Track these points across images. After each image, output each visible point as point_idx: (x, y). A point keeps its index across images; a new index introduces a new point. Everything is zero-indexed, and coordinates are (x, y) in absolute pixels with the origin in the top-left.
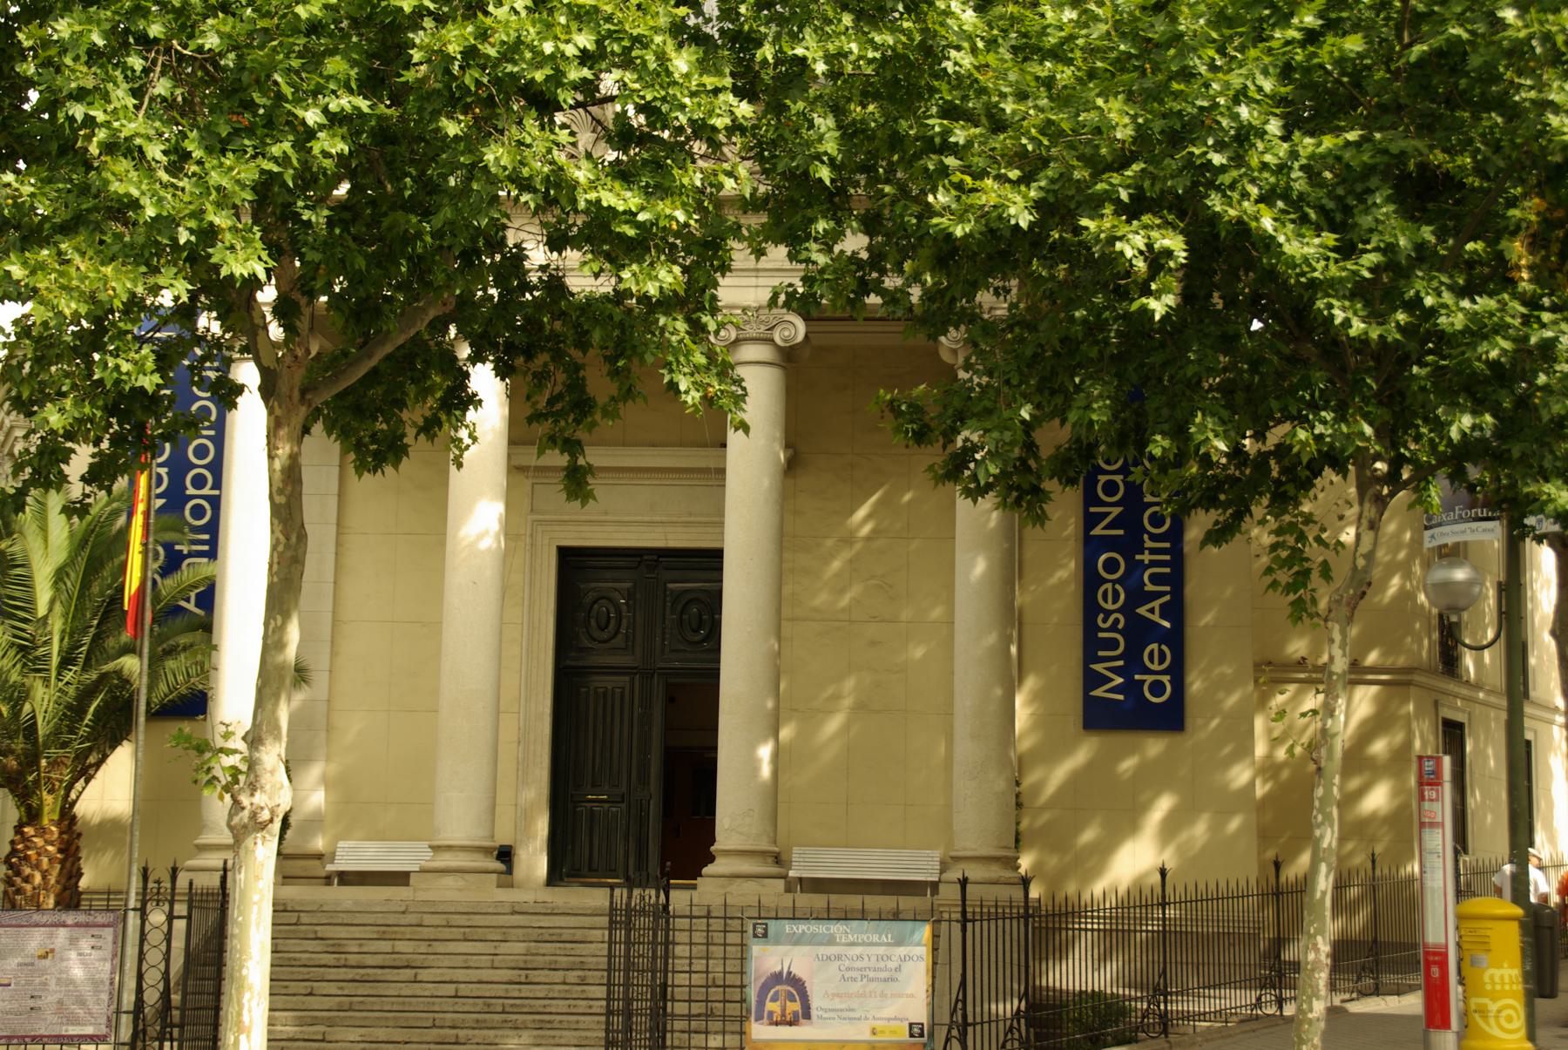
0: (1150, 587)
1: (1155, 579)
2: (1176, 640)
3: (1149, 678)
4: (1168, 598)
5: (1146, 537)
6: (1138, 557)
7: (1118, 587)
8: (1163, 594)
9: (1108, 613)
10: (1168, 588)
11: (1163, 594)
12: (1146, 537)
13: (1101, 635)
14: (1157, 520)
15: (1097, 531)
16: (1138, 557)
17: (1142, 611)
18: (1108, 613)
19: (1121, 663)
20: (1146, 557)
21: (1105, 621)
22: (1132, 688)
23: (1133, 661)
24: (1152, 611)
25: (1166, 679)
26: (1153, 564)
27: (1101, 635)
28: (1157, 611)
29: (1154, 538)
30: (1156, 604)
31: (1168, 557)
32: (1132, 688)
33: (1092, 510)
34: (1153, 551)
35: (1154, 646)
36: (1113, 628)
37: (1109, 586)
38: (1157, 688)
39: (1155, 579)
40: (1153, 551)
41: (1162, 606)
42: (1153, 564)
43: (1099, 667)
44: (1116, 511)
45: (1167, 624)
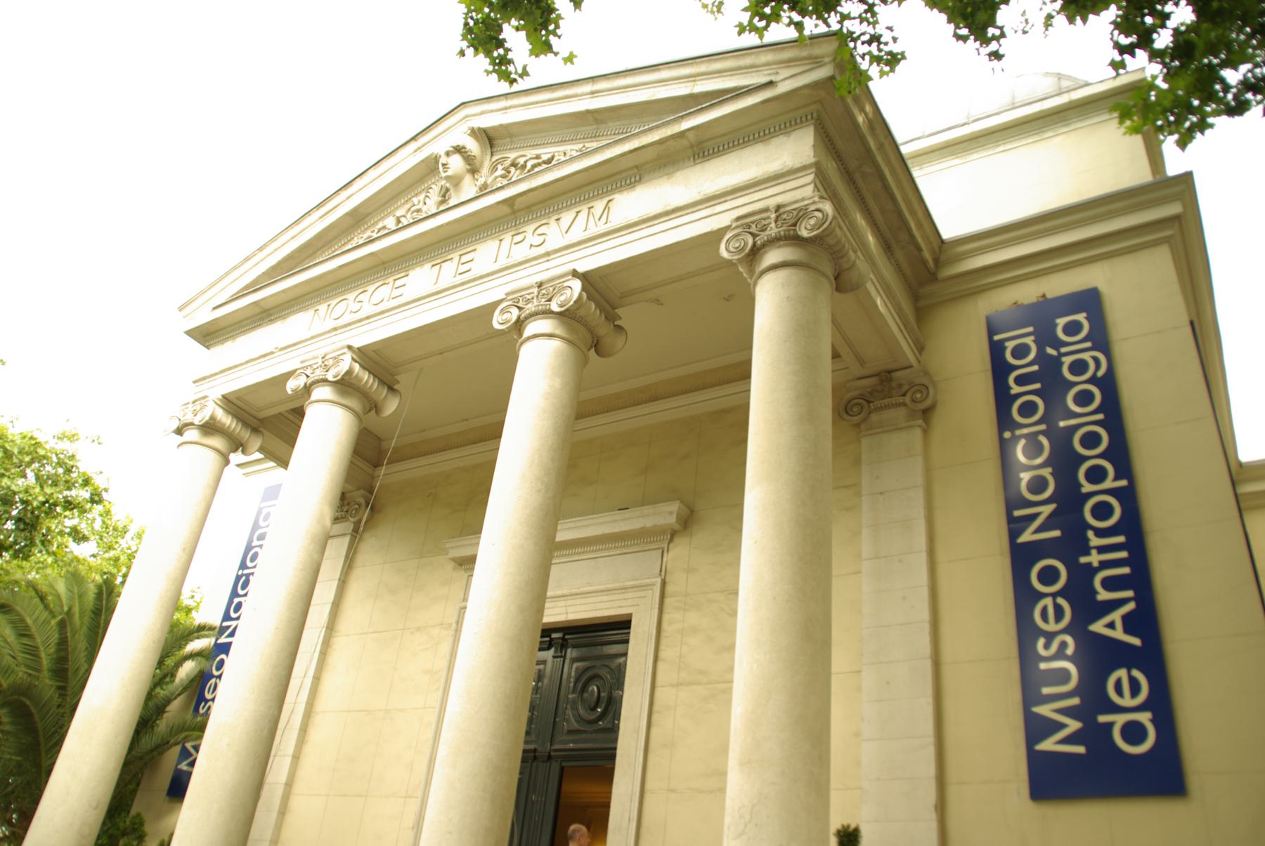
0: (1103, 595)
1: (1109, 584)
2: (1150, 657)
3: (1120, 720)
4: (1131, 606)
5: (1090, 534)
6: (1083, 560)
7: (1060, 601)
8: (1123, 602)
9: (1050, 637)
10: (1130, 594)
11: (1123, 602)
12: (1090, 534)
13: (1043, 666)
14: (1102, 511)
15: (1026, 537)
16: (1083, 560)
17: (1098, 627)
18: (1050, 637)
19: (1075, 701)
20: (1094, 559)
21: (1047, 646)
22: (1094, 735)
23: (1094, 699)
24: (1111, 625)
25: (1145, 718)
26: (1104, 565)
27: (1043, 666)
28: (1119, 625)
29: (1100, 533)
30: (1116, 616)
31: (1123, 554)
32: (1094, 735)
33: (1017, 513)
34: (1102, 550)
35: (1122, 673)
36: (1060, 655)
37: (1048, 601)
38: (1134, 732)
39: (1109, 584)
40: (1102, 550)
41: (1125, 618)
42: (1104, 565)
43: (1044, 710)
44: (1047, 510)
45: (1136, 641)
